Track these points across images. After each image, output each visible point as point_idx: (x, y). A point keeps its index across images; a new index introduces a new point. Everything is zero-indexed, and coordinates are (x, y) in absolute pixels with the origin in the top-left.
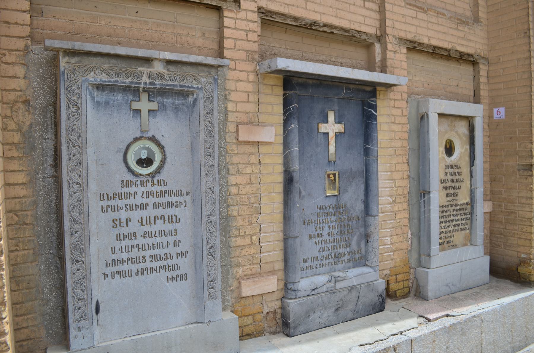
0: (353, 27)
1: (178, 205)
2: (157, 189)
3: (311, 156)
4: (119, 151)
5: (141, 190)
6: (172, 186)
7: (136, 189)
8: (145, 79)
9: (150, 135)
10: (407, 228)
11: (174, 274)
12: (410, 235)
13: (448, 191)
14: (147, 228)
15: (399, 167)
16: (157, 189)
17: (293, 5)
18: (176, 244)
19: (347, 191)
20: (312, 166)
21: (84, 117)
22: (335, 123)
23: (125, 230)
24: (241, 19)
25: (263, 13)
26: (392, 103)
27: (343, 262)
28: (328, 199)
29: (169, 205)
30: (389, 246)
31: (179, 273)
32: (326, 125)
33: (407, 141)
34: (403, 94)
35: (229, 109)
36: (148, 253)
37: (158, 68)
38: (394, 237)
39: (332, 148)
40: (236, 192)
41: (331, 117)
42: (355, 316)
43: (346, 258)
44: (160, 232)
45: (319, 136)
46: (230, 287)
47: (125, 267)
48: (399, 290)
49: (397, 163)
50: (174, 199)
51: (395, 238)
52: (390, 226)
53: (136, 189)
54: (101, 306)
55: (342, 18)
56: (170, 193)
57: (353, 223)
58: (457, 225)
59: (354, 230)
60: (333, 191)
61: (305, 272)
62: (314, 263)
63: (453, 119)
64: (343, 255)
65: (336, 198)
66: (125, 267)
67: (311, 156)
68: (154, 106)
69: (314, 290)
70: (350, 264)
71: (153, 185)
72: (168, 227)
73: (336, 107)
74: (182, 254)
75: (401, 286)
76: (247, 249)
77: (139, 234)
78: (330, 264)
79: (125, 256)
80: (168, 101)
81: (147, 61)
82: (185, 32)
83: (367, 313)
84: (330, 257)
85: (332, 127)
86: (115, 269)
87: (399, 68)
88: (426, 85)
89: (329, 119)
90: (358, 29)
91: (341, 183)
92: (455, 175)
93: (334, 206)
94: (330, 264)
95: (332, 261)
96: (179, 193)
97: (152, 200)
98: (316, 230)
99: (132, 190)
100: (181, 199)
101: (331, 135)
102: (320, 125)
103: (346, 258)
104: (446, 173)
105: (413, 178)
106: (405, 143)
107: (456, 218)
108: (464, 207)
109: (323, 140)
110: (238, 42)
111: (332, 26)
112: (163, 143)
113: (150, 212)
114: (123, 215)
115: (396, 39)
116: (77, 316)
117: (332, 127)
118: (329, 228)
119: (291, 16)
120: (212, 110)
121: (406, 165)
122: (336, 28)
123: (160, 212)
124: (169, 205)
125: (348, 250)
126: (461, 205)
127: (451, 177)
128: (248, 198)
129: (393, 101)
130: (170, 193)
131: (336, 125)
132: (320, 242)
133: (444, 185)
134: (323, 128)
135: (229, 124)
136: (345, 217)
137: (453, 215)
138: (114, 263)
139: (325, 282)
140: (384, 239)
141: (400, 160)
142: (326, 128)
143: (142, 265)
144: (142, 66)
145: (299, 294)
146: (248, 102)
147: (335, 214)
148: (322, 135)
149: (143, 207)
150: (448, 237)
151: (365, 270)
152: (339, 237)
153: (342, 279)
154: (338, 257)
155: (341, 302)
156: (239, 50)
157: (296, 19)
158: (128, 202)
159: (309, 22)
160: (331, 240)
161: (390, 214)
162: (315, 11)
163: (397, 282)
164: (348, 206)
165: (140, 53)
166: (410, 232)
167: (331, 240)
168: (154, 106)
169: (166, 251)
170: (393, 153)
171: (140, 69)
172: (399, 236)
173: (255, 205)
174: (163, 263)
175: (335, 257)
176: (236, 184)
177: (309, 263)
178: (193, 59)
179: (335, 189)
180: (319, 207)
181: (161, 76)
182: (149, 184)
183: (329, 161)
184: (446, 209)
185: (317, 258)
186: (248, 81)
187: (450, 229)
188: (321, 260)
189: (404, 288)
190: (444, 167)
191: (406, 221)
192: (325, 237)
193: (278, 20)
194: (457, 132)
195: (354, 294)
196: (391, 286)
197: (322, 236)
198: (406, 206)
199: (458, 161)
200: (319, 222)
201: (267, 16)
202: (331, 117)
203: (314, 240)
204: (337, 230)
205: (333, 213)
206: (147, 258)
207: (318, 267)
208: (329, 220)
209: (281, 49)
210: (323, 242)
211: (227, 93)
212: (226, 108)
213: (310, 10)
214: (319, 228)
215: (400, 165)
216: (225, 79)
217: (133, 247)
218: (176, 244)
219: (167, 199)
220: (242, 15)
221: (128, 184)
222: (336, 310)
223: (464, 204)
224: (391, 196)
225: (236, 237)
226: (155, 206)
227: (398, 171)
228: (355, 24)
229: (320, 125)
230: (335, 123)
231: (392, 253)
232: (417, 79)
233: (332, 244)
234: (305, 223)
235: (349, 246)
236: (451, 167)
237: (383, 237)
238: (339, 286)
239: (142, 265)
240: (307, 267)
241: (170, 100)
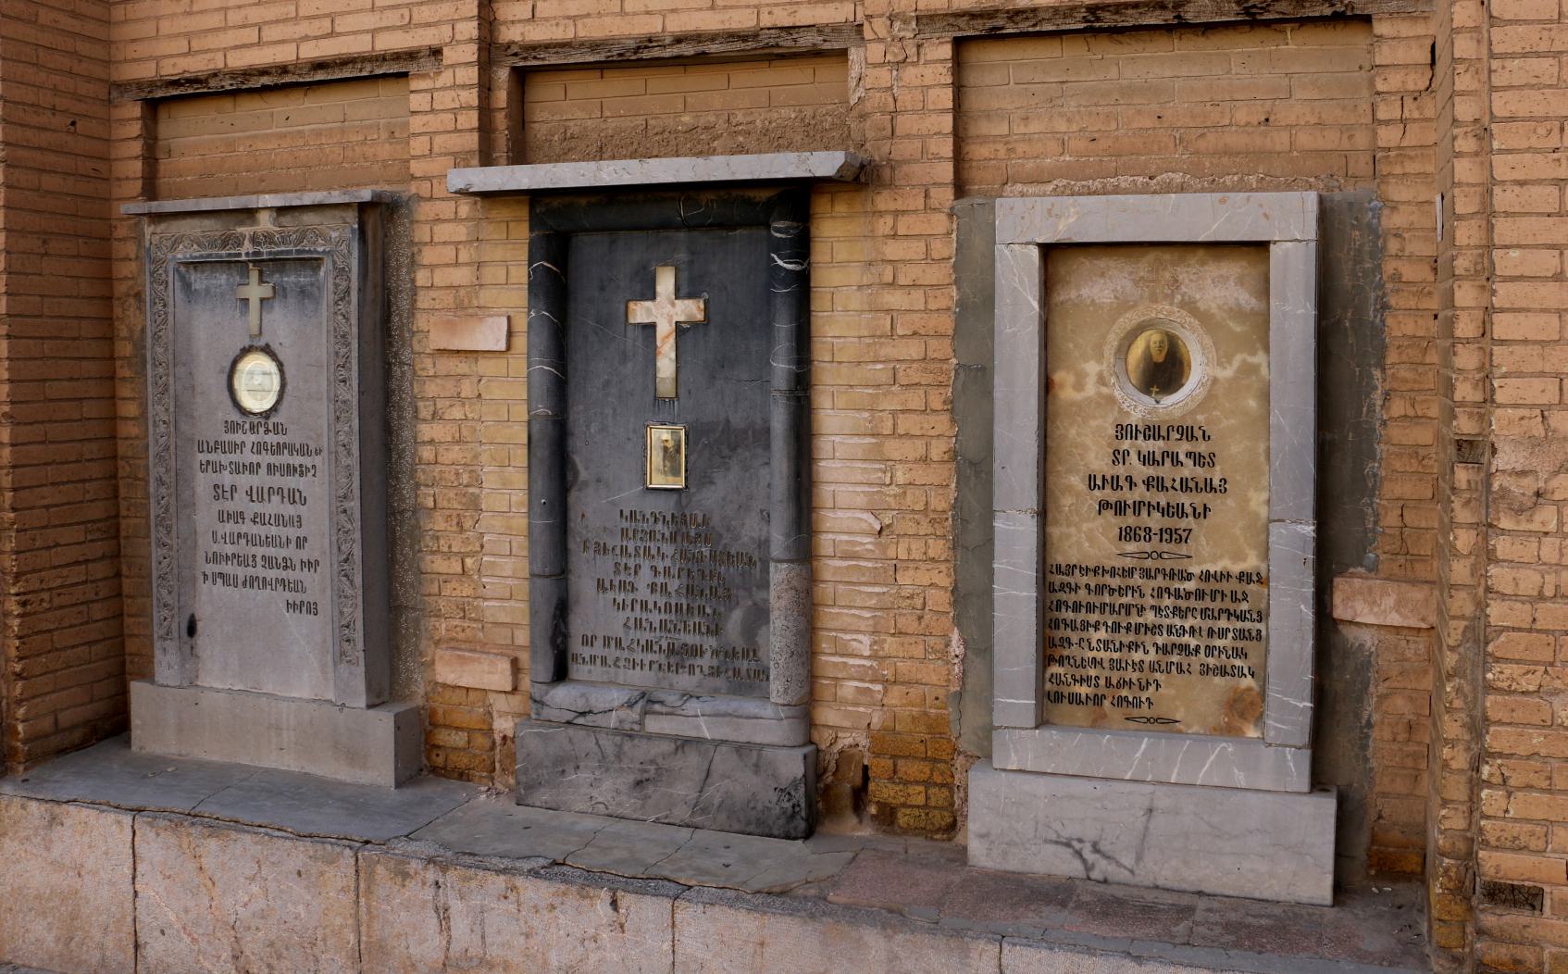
0: (766, 21)
1: (302, 471)
2: (272, 439)
3: (607, 384)
4: (222, 371)
5: (250, 438)
6: (292, 437)
7: (243, 437)
8: (247, 247)
9: (262, 343)
10: (947, 621)
11: (298, 597)
12: (956, 647)
13: (1130, 520)
14: (258, 507)
15: (905, 424)
16: (272, 439)
17: (588, 15)
18: (301, 542)
19: (712, 483)
20: (609, 411)
21: (171, 318)
22: (677, 298)
23: (230, 506)
24: (443, 89)
25: (515, 54)
26: (884, 226)
27: (697, 670)
28: (651, 498)
29: (290, 470)
30: (867, 663)
31: (305, 597)
32: (648, 304)
33: (947, 341)
34: (933, 191)
35: (419, 283)
36: (260, 551)
37: (265, 223)
38: (889, 639)
39: (666, 365)
40: (432, 458)
41: (666, 282)
42: (698, 819)
43: (706, 661)
44: (277, 517)
45: (630, 333)
46: (421, 655)
47: (228, 568)
48: (904, 805)
49: (903, 411)
50: (296, 460)
51: (890, 644)
52: (873, 602)
53: (243, 437)
54: (200, 625)
55: (732, 7)
56: (291, 449)
57: (731, 572)
58: (1184, 649)
59: (734, 591)
60: (670, 478)
61: (587, 667)
62: (612, 653)
63: (1166, 256)
64: (696, 651)
65: (675, 496)
66: (228, 568)
67: (607, 384)
68: (265, 291)
69: (583, 714)
70: (719, 682)
71: (267, 431)
72: (289, 510)
73: (682, 256)
74: (311, 565)
75: (917, 795)
76: (454, 584)
77: (249, 515)
78: (655, 666)
79: (229, 549)
80: (290, 279)
81: (249, 213)
82: (361, 138)
83: (737, 827)
84: (656, 648)
85: (666, 309)
86: (217, 568)
87: (914, 111)
88: (1078, 144)
89: (659, 289)
90: (787, 22)
91: (692, 458)
92: (1176, 461)
93: (669, 518)
94: (655, 666)
95: (662, 659)
96: (304, 450)
97: (266, 458)
98: (617, 572)
99: (238, 437)
100: (307, 461)
101: (665, 330)
102: (632, 305)
103: (706, 661)
104: (1119, 457)
105: (972, 464)
106: (942, 348)
107: (1177, 622)
108: (1226, 586)
109: (639, 343)
110: (438, 140)
111: (699, 36)
112: (281, 358)
113: (262, 479)
114: (227, 479)
115: (905, 22)
116: (162, 632)
117: (666, 309)
118: (654, 573)
119: (582, 44)
120: (348, 291)
121: (945, 418)
122: (713, 37)
123: (277, 480)
124: (290, 470)
125: (710, 642)
126: (1207, 576)
127: (1151, 471)
128: (457, 474)
129: (889, 220)
130: (291, 449)
131: (678, 302)
132: (628, 602)
133: (1109, 494)
134: (640, 312)
135: (418, 315)
136: (706, 551)
137: (1157, 610)
138: (216, 558)
139: (616, 704)
140: (848, 637)
141: (915, 400)
142: (649, 311)
143: (250, 571)
144: (242, 224)
145: (546, 713)
146: (457, 264)
147: (673, 538)
148: (638, 332)
149: (253, 468)
150: (1123, 683)
151: (750, 706)
152: (684, 601)
153: (664, 709)
154: (680, 656)
155: (652, 768)
156: (440, 155)
157: (594, 46)
158: (234, 457)
159: (632, 44)
160: (661, 604)
161: (870, 565)
162: (648, 13)
163: (893, 775)
164: (716, 521)
165: (232, 203)
166: (955, 636)
167: (661, 604)
168: (265, 291)
169: (283, 553)
170: (885, 377)
171: (240, 230)
172: (913, 639)
173: (471, 490)
174: (282, 574)
175: (672, 650)
176: (432, 442)
177: (598, 650)
178: (308, 198)
179: (675, 472)
180: (627, 513)
181: (269, 238)
182: (262, 430)
183: (656, 398)
184: (1115, 582)
185: (619, 643)
186: (456, 219)
187: (1137, 656)
188: (632, 650)
189: (926, 806)
190: (1112, 432)
191: (939, 600)
192: (643, 593)
193: (553, 60)
194: (1190, 306)
195: (692, 760)
196: (872, 786)
197: (633, 589)
198: (938, 548)
199: (1193, 412)
200: (624, 550)
201: (525, 59)
202: (666, 282)
203: (610, 595)
204: (677, 582)
205: (667, 535)
206: (258, 559)
207: (621, 663)
208: (654, 552)
209: (589, 123)
210: (638, 607)
211: (415, 249)
212: (413, 281)
213: (635, 14)
214: (626, 568)
215: (914, 417)
216: (412, 222)
217: (239, 535)
218: (301, 542)
219: (285, 459)
220: (446, 78)
221: (232, 427)
222: (639, 783)
223: (1225, 576)
224: (872, 511)
225: (433, 553)
226: (271, 469)
227: (907, 435)
228: (775, 10)
229: (632, 305)
230: (677, 298)
231: (879, 687)
232: (1034, 127)
233: (663, 617)
234: (586, 548)
235: (715, 630)
236: (1152, 432)
237: (844, 631)
238: (653, 725)
239: (250, 571)
240: (593, 659)
241: (293, 278)
